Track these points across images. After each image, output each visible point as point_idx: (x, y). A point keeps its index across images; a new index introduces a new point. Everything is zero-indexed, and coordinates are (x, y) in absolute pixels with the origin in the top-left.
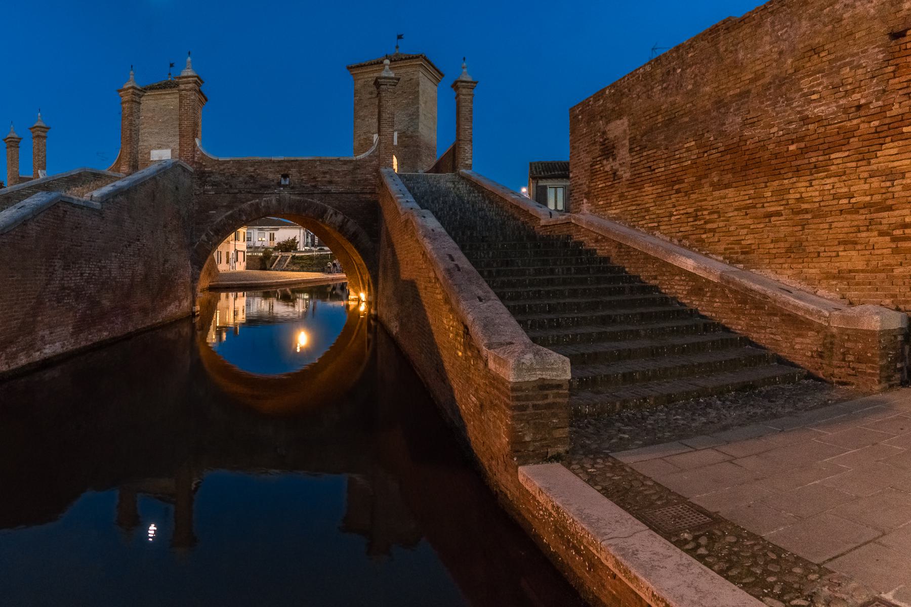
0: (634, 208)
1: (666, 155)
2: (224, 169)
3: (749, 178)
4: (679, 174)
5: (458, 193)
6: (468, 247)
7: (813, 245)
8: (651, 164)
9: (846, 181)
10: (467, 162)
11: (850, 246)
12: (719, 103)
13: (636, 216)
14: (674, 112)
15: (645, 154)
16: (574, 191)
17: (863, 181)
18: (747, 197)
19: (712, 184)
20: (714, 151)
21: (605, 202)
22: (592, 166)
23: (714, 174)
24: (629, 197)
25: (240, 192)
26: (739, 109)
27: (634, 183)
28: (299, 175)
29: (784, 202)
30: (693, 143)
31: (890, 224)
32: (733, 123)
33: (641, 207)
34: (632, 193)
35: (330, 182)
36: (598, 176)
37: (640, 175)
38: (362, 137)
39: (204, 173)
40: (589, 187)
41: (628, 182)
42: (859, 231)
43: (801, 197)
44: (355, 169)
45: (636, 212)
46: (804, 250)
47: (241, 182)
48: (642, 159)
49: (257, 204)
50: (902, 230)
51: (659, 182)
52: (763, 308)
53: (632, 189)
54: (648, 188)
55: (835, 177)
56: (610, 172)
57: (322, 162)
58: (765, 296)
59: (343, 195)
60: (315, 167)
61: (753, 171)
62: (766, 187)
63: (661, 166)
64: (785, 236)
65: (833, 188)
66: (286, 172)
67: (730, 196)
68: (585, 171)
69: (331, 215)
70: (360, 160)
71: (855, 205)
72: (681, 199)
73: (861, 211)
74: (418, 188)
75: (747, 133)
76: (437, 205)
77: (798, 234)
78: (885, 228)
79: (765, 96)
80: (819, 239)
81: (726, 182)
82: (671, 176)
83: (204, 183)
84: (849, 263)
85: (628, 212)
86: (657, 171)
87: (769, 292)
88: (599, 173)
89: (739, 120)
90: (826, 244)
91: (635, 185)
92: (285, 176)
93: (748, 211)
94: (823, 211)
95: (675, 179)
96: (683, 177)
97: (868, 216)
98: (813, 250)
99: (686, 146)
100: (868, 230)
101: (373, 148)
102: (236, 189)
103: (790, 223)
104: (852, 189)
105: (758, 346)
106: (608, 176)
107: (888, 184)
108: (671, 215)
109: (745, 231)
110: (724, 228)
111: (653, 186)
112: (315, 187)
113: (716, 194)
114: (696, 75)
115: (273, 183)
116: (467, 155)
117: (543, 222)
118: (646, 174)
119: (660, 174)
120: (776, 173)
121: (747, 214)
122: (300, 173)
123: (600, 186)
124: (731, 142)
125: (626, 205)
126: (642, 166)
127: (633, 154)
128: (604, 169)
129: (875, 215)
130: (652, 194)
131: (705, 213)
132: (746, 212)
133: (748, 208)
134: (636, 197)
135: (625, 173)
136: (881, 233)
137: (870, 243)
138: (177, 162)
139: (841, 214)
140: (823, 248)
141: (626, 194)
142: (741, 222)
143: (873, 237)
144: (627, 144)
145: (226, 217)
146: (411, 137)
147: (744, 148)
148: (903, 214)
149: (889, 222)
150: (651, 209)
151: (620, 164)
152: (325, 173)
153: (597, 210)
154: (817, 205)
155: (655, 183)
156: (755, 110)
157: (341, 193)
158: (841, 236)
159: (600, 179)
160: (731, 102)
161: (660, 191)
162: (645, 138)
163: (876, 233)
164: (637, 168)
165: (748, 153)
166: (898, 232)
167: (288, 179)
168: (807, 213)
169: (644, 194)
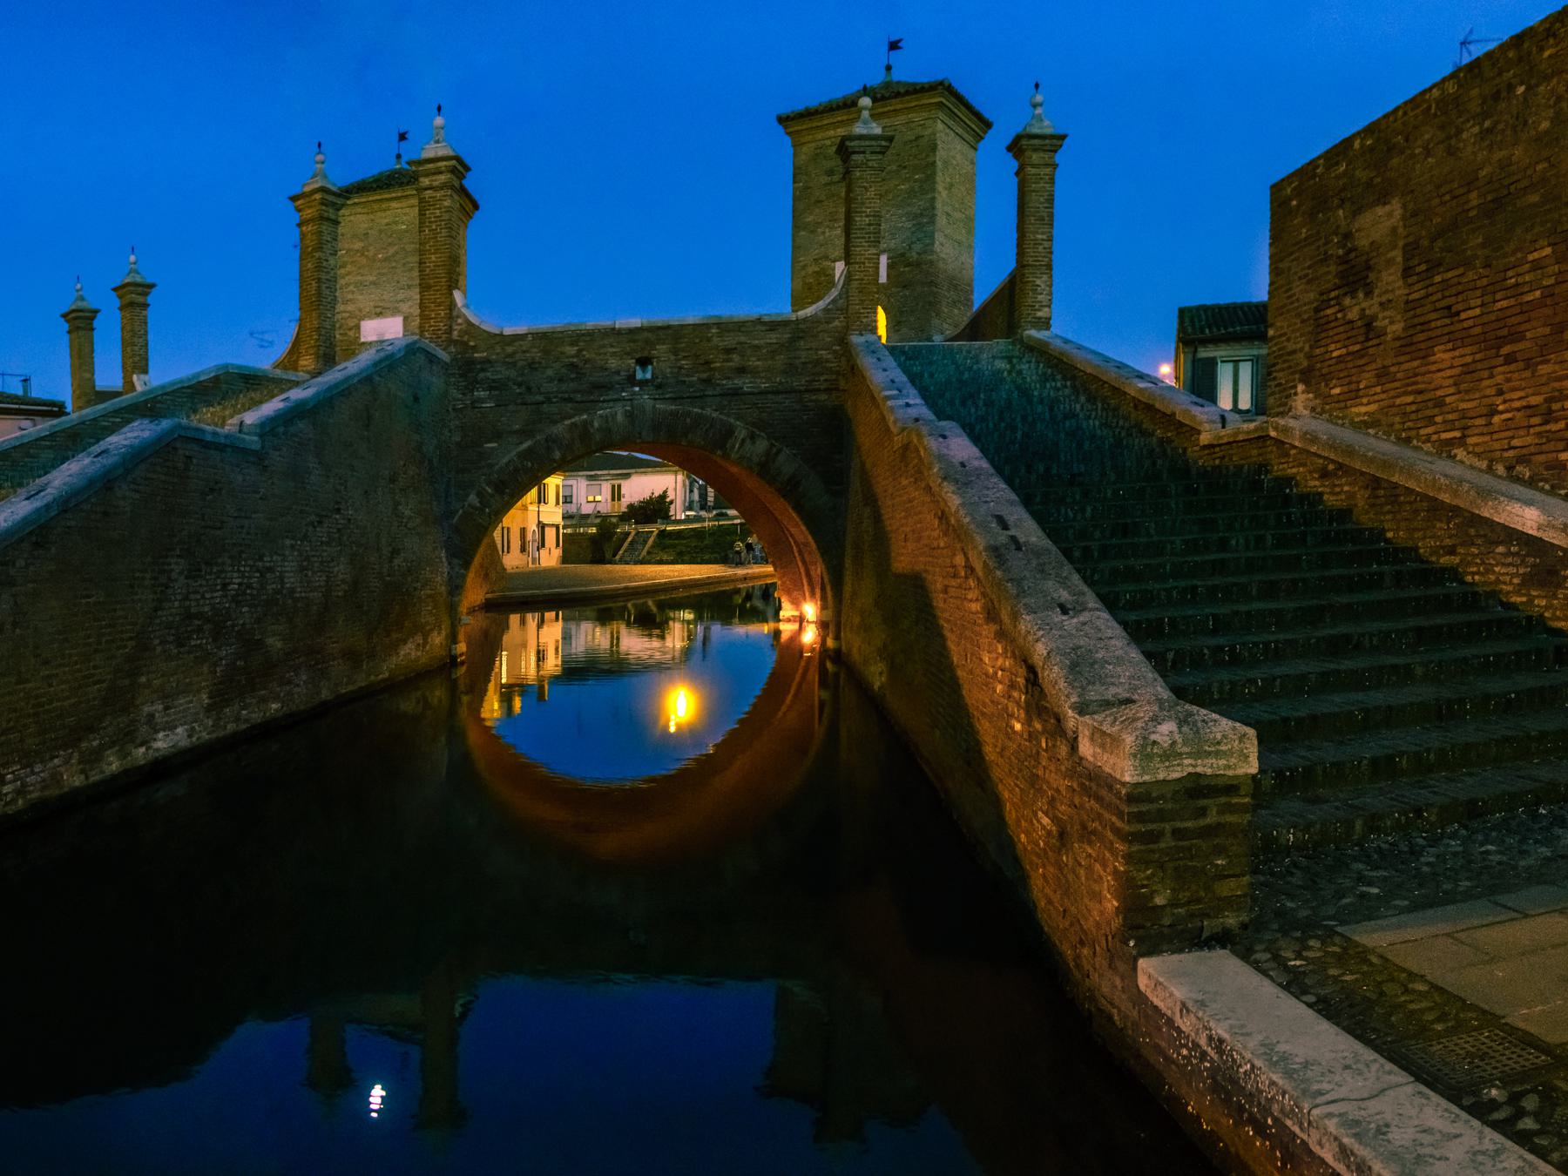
1: (1485, 282)
2: (514, 353)
4: (1514, 320)
5: (1020, 381)
6: (1038, 499)
8: (1453, 300)
10: (1039, 314)
15: (1438, 279)
16: (1277, 368)
21: (1345, 389)
24: (1399, 376)
25: (549, 400)
27: (1412, 344)
28: (673, 358)
30: (1548, 251)
35: (741, 371)
36: (1331, 333)
37: (1426, 327)
38: (810, 270)
39: (471, 363)
40: (1310, 357)
41: (1398, 344)
44: (793, 340)
47: (551, 380)
48: (1431, 289)
49: (585, 423)
53: (1407, 357)
54: (1442, 355)
56: (1359, 323)
57: (724, 327)
59: (770, 396)
60: (709, 340)
63: (1473, 305)
66: (645, 354)
68: (1303, 321)
69: (743, 441)
70: (805, 320)
74: (931, 375)
76: (973, 410)
82: (1494, 326)
83: (472, 386)
86: (1463, 316)
88: (1333, 324)
91: (1413, 348)
92: (644, 362)
95: (1505, 332)
96: (1523, 327)
99: (1530, 258)
101: (834, 293)
102: (541, 394)
111: (1454, 349)
112: (708, 381)
115: (617, 378)
116: (1040, 297)
117: (1205, 439)
118: (1439, 323)
119: (1470, 323)
122: (675, 353)
123: (1335, 354)
126: (1430, 307)
127: (1410, 280)
128: (1345, 316)
130: (1452, 367)
134: (1416, 375)
135: (1392, 323)
138: (415, 342)
141: (1392, 369)
145: (519, 455)
146: (918, 264)
151: (1381, 304)
152: (728, 351)
153: (1328, 407)
155: (1459, 343)
157: (762, 393)
159: (1336, 338)
161: (1469, 359)
164: (1418, 311)
167: (650, 367)
169: (1433, 368)
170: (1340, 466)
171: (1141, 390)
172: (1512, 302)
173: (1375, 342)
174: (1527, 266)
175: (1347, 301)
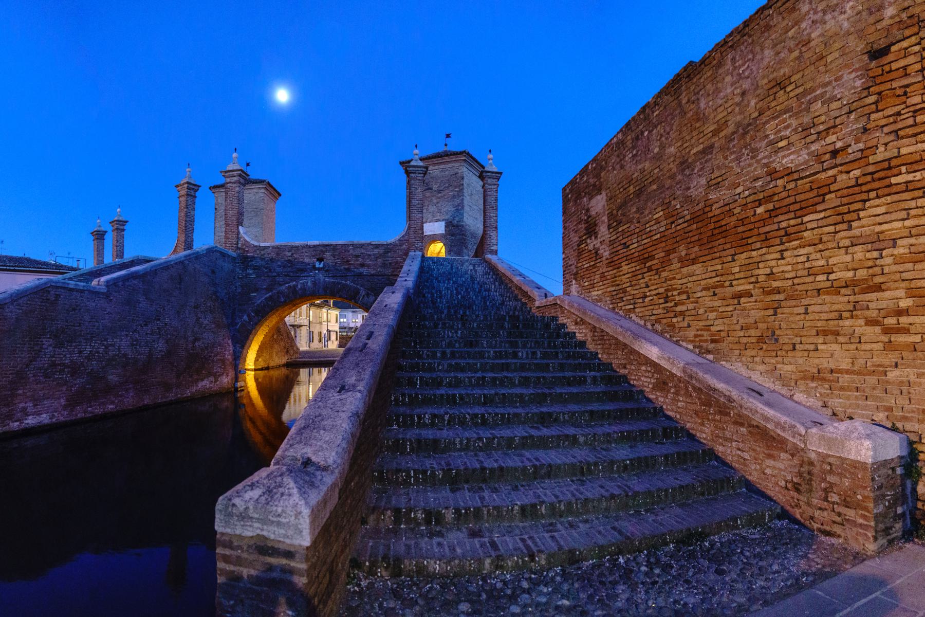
0: (613, 289)
1: (637, 230)
3: (716, 250)
4: (650, 249)
7: (787, 335)
9: (823, 251)
11: (830, 338)
12: (684, 165)
13: (615, 297)
14: (644, 180)
15: (620, 229)
17: (843, 251)
18: (714, 274)
19: (681, 260)
20: (680, 221)
21: (589, 283)
22: (579, 245)
23: (681, 248)
24: (608, 277)
26: (702, 169)
27: (613, 262)
29: (753, 279)
30: (661, 213)
31: (879, 310)
32: (698, 186)
33: (620, 287)
34: (611, 273)
41: (607, 261)
42: (841, 318)
43: (772, 273)
45: (615, 293)
46: (777, 340)
48: (618, 235)
50: (895, 318)
51: (633, 260)
52: (728, 414)
53: (611, 268)
54: (625, 268)
55: (810, 246)
56: (593, 252)
58: (731, 400)
61: (719, 242)
62: (734, 260)
64: (756, 323)
65: (808, 260)
67: (697, 272)
71: (834, 282)
72: (652, 277)
73: (843, 291)
75: (712, 196)
77: (769, 320)
78: (874, 315)
79: (728, 149)
80: (793, 326)
81: (693, 256)
82: (643, 252)
84: (830, 360)
85: (607, 294)
86: (631, 247)
87: (734, 394)
89: (703, 181)
90: (802, 334)
91: (613, 264)
93: (717, 291)
94: (797, 290)
95: (646, 256)
97: (852, 298)
98: (786, 341)
99: (655, 217)
100: (852, 317)
103: (760, 305)
104: (831, 261)
105: (724, 463)
106: (592, 256)
107: (876, 254)
108: (646, 297)
109: (712, 315)
110: (693, 311)
113: (685, 270)
114: (662, 136)
118: (622, 251)
119: (633, 251)
120: (744, 244)
121: (715, 295)
123: (585, 266)
124: (697, 208)
125: (606, 286)
126: (618, 243)
127: (611, 230)
129: (860, 297)
131: (675, 293)
132: (714, 292)
133: (716, 287)
134: (615, 277)
136: (870, 321)
137: (856, 335)
139: (819, 295)
140: (798, 339)
142: (710, 304)
143: (858, 326)
144: (606, 220)
147: (710, 215)
148: (896, 296)
149: (878, 307)
150: (628, 289)
154: (790, 282)
155: (630, 261)
156: (719, 168)
158: (819, 324)
160: (695, 161)
161: (634, 269)
162: (620, 212)
163: (862, 322)
164: (615, 246)
165: (713, 220)
166: (891, 321)
168: (779, 293)
169: (621, 273)
170: (582, 320)
171: (517, 281)
172: (649, 240)
173: (599, 260)
174: (653, 222)
175: (589, 241)
